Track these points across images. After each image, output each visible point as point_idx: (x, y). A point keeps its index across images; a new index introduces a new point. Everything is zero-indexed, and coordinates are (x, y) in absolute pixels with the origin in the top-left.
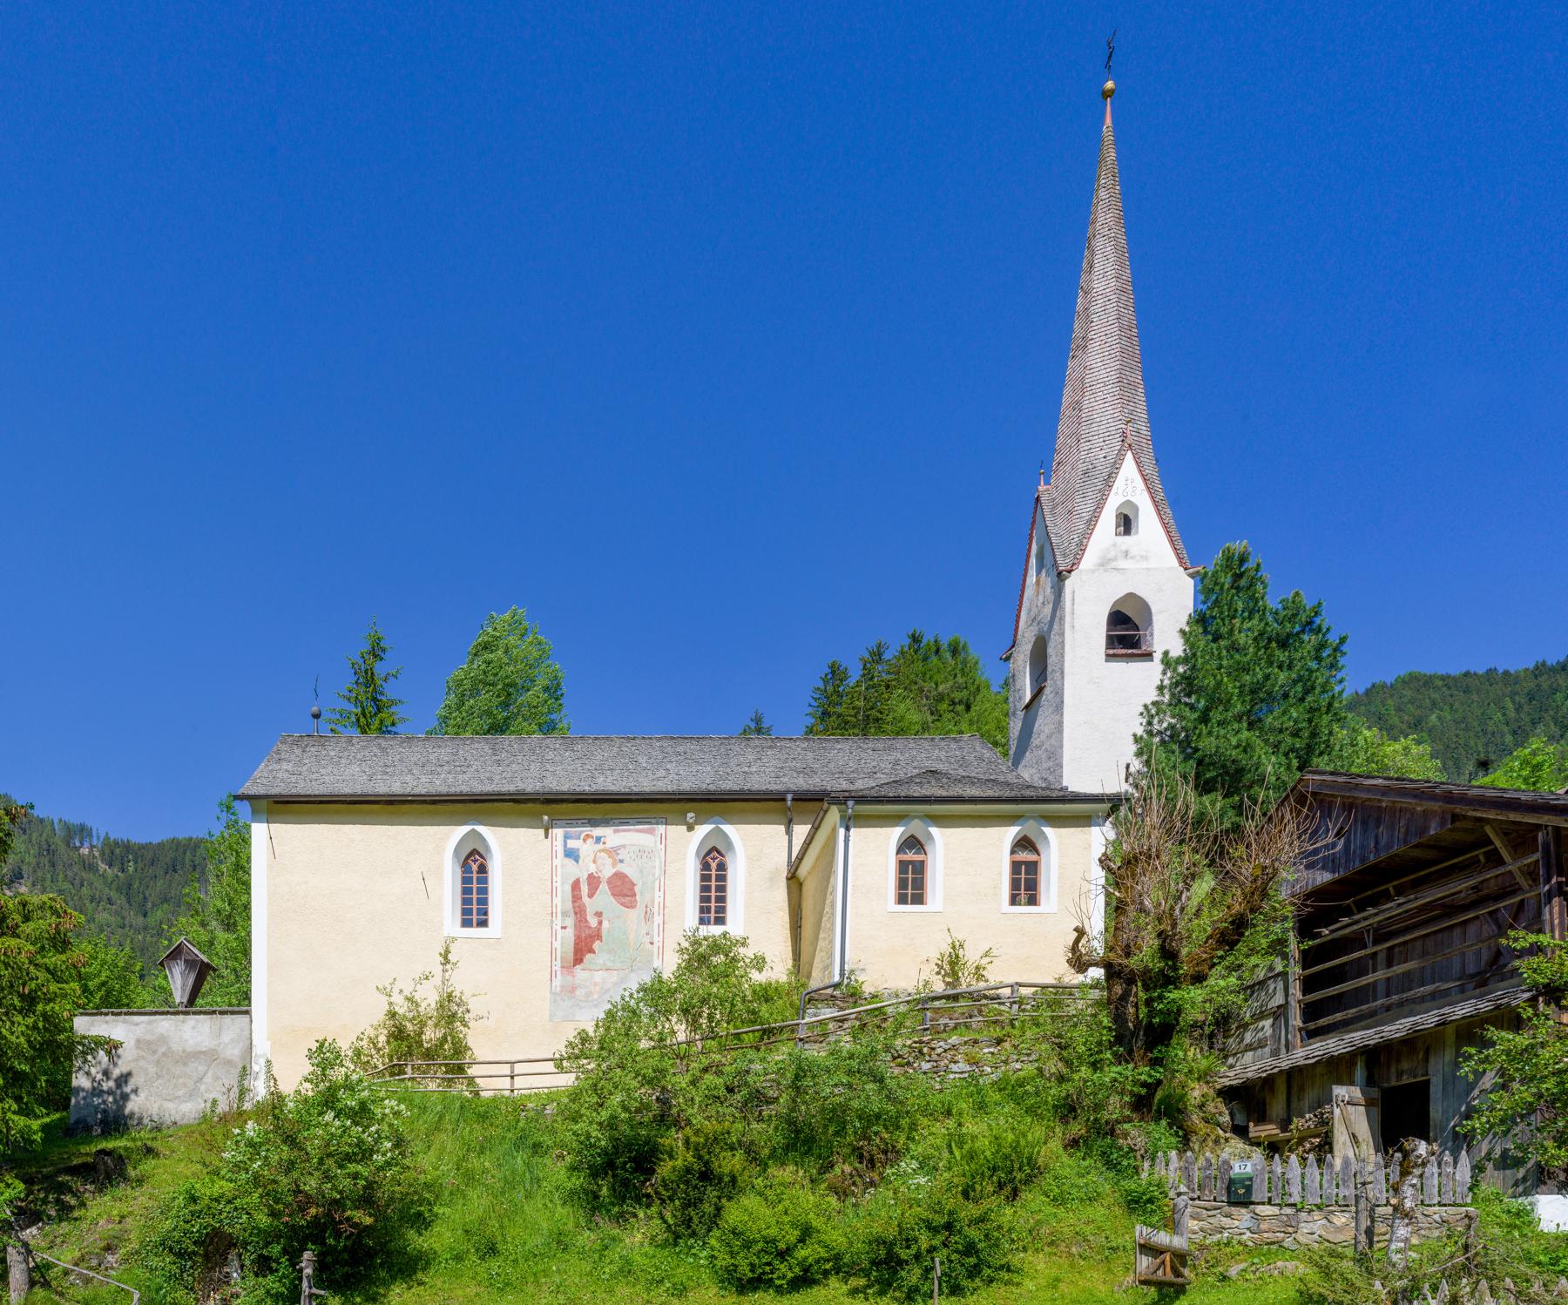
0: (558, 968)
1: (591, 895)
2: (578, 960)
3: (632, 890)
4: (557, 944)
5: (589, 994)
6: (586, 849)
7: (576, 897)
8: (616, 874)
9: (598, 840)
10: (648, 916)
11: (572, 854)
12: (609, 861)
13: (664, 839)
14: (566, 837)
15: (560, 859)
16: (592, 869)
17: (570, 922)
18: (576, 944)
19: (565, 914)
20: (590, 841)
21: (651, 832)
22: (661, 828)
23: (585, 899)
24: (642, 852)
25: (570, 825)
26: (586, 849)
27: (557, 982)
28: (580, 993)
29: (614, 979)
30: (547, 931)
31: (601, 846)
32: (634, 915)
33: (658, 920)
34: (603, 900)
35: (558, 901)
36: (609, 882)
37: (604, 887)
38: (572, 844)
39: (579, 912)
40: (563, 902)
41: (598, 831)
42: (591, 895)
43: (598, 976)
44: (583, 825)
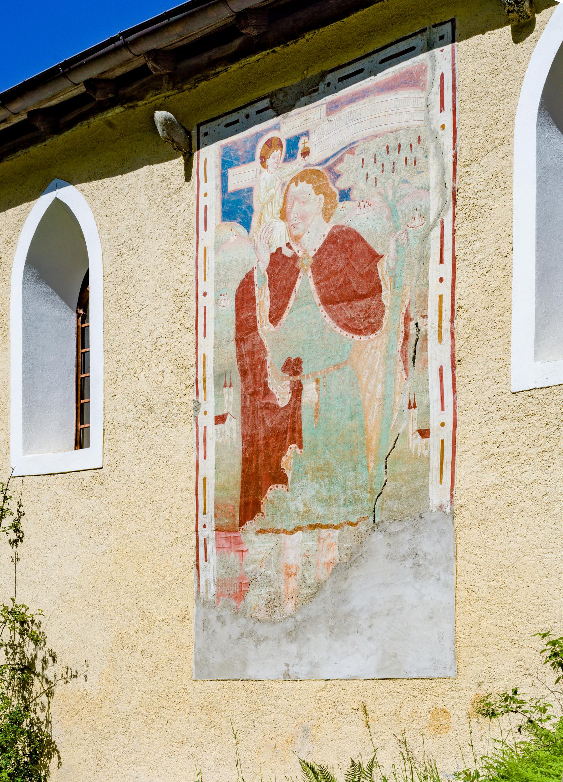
0: (208, 533)
1: (275, 317)
2: (250, 508)
3: (371, 275)
4: (208, 469)
5: (273, 603)
6: (263, 180)
7: (245, 328)
8: (332, 239)
9: (292, 148)
10: (412, 351)
11: (237, 209)
12: (315, 203)
13: (449, 90)
14: (227, 163)
15: (215, 227)
16: (279, 236)
17: (232, 400)
18: (246, 461)
19: (222, 382)
20: (276, 156)
21: (412, 81)
22: (438, 59)
23: (265, 328)
24: (402, 152)
25: (234, 127)
26: (263, 180)
27: (210, 572)
28: (255, 597)
29: (333, 555)
30: (185, 436)
31: (298, 165)
32: (383, 343)
33: (437, 354)
34: (305, 326)
35: (207, 346)
36: (318, 267)
37: (306, 284)
38: (239, 178)
39: (251, 365)
40: (218, 346)
41: (289, 124)
42: (275, 317)
43: (296, 546)
44: (261, 116)
